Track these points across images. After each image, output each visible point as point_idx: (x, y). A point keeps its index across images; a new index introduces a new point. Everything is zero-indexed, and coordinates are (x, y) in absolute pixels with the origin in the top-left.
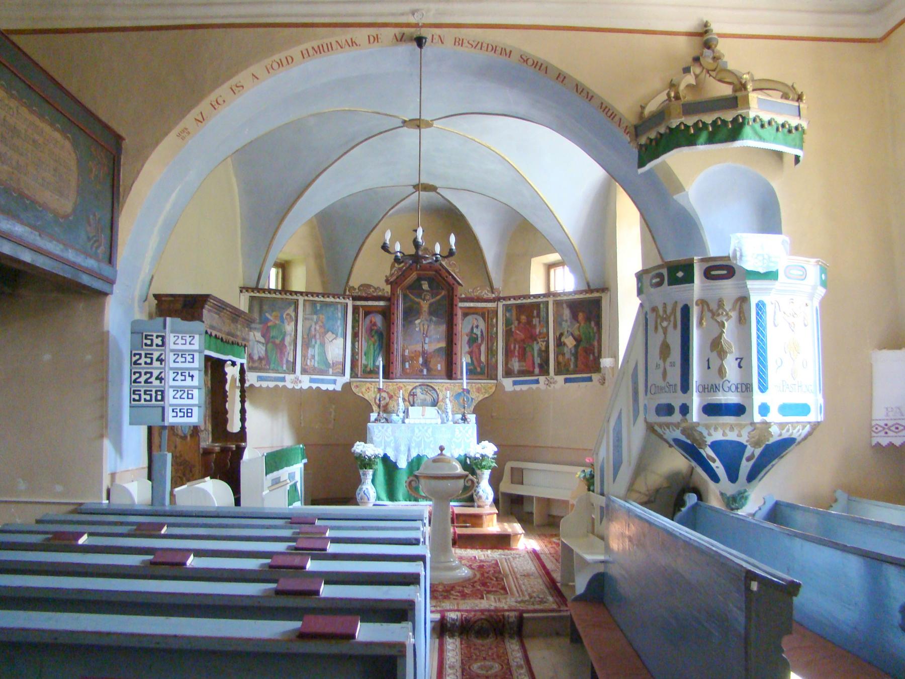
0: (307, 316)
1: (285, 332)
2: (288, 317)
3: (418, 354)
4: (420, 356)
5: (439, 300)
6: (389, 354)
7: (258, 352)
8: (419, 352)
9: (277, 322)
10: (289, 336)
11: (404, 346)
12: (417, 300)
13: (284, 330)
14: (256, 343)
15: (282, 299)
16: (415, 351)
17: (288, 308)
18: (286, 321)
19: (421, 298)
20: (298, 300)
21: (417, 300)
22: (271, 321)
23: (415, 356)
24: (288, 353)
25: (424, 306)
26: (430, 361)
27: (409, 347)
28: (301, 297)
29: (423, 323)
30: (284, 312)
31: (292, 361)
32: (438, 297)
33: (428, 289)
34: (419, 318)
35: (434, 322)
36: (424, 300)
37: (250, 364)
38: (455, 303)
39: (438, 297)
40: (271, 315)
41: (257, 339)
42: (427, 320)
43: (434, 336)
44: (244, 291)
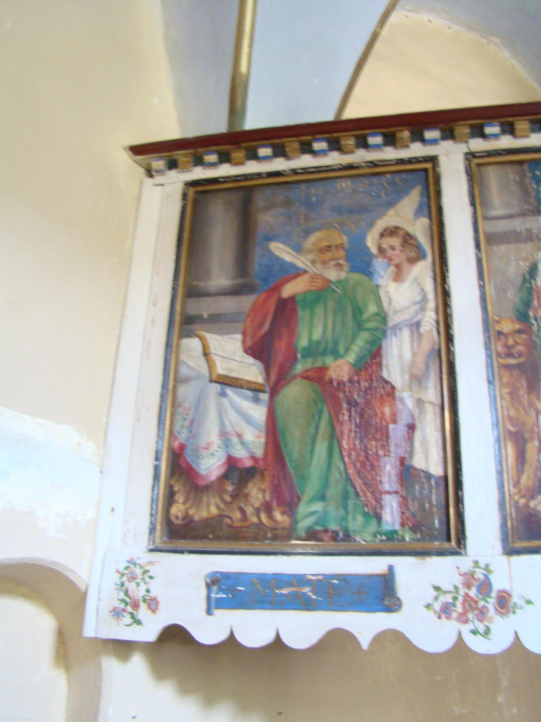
0: (500, 226)
1: (383, 317)
2: (395, 241)
7: (224, 435)
9: (332, 274)
10: (406, 333)
13: (372, 309)
14: (216, 388)
15: (350, 167)
17: (391, 204)
18: (379, 264)
20: (433, 159)
22: (298, 273)
24: (411, 428)
28: (448, 144)
30: (371, 225)
31: (436, 470)
37: (177, 510)
40: (298, 249)
41: (221, 369)
44: (158, 164)
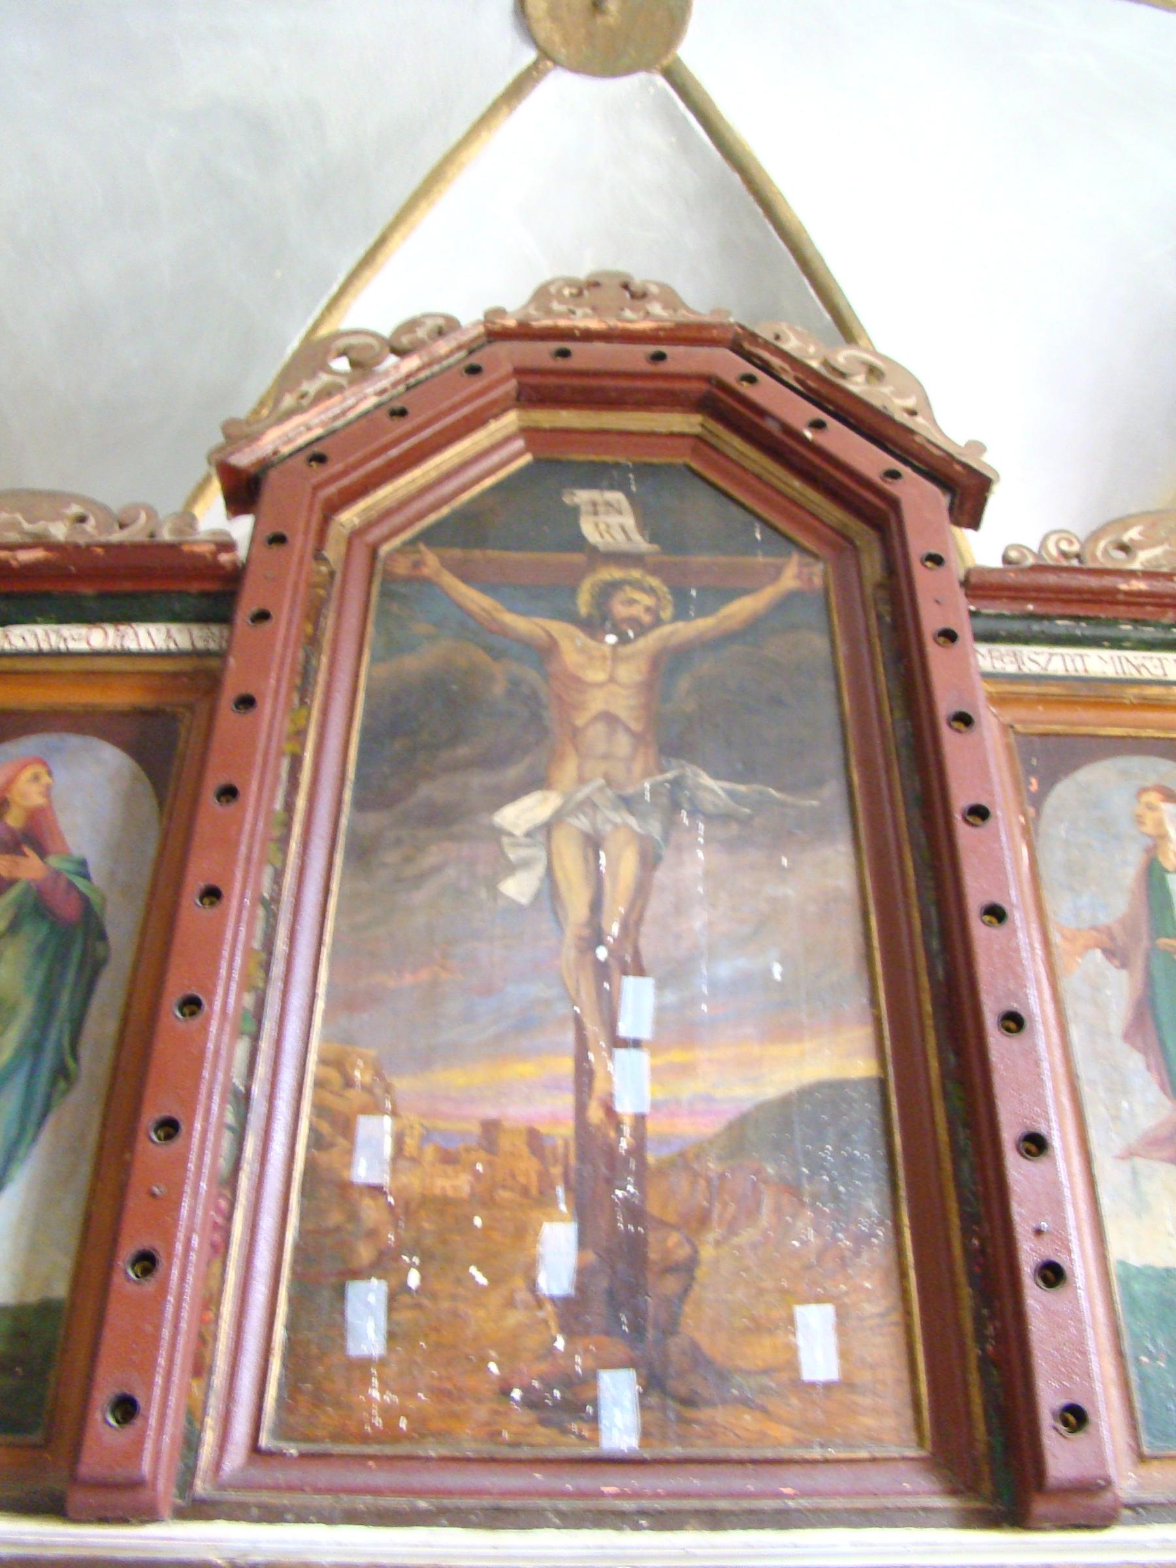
3: (528, 1167)
4: (543, 1200)
5: (753, 628)
6: (128, 1139)
8: (534, 1139)
11: (336, 1062)
12: (520, 624)
16: (491, 1128)
19: (572, 618)
21: (520, 624)
23: (485, 1199)
25: (596, 675)
26: (688, 1268)
27: (403, 1084)
29: (582, 822)
32: (742, 608)
33: (641, 544)
34: (537, 782)
35: (723, 818)
36: (594, 625)
38: (931, 620)
39: (742, 608)
42: (628, 803)
43: (725, 970)
